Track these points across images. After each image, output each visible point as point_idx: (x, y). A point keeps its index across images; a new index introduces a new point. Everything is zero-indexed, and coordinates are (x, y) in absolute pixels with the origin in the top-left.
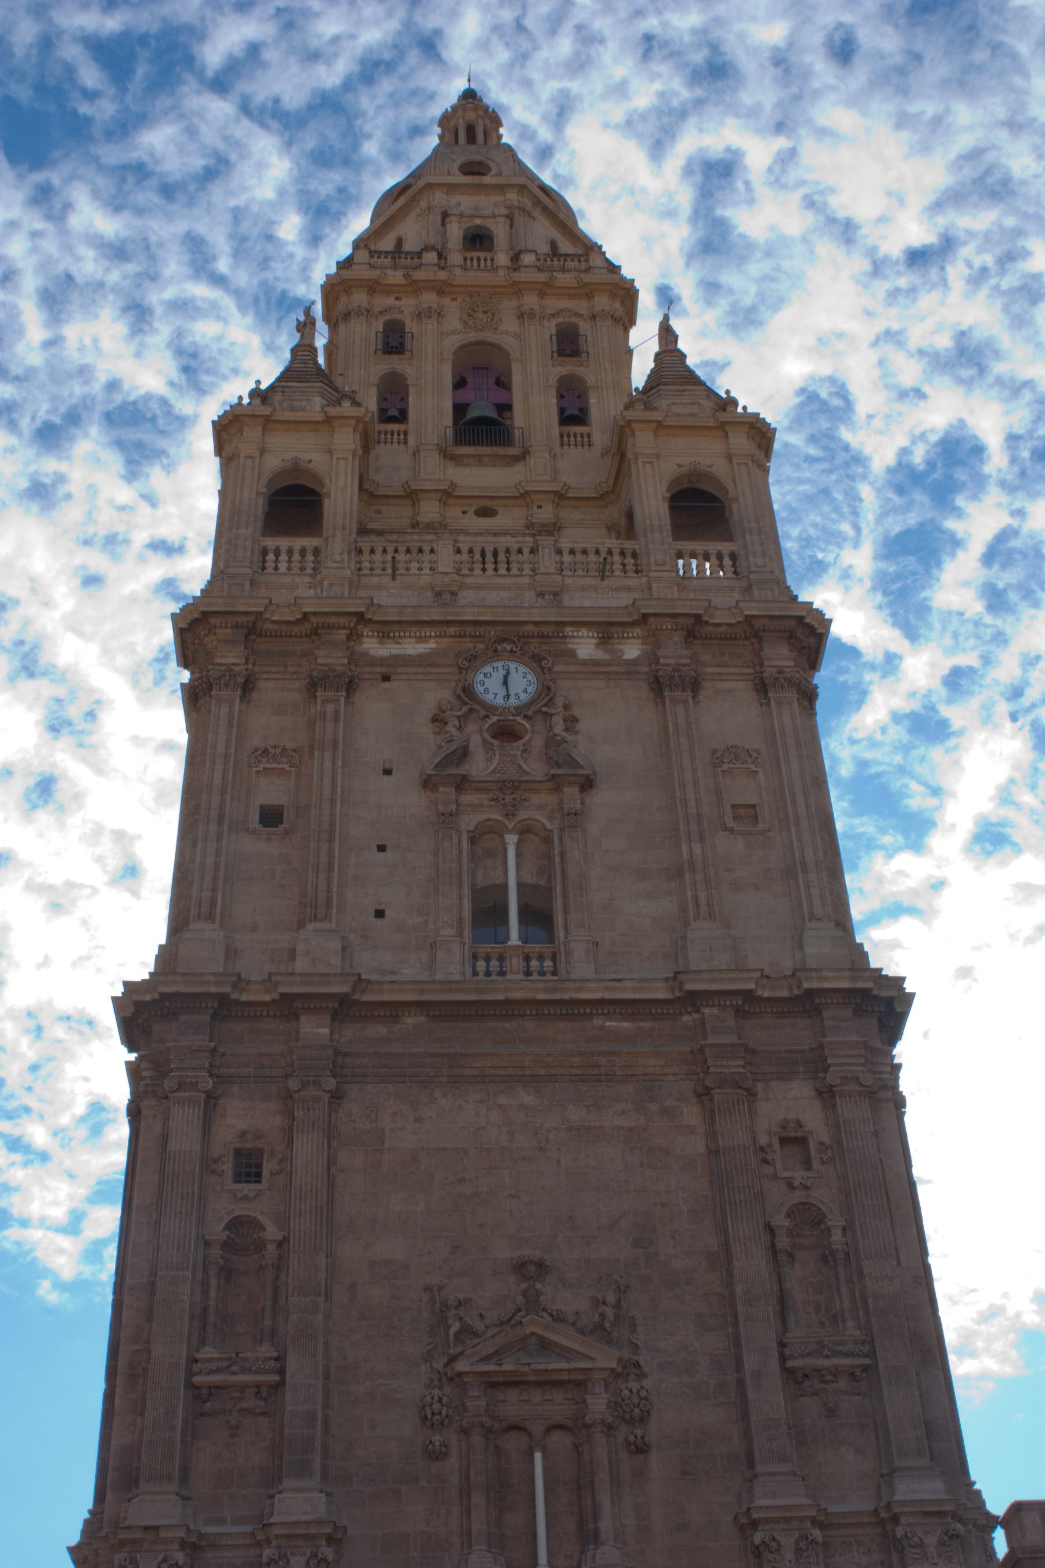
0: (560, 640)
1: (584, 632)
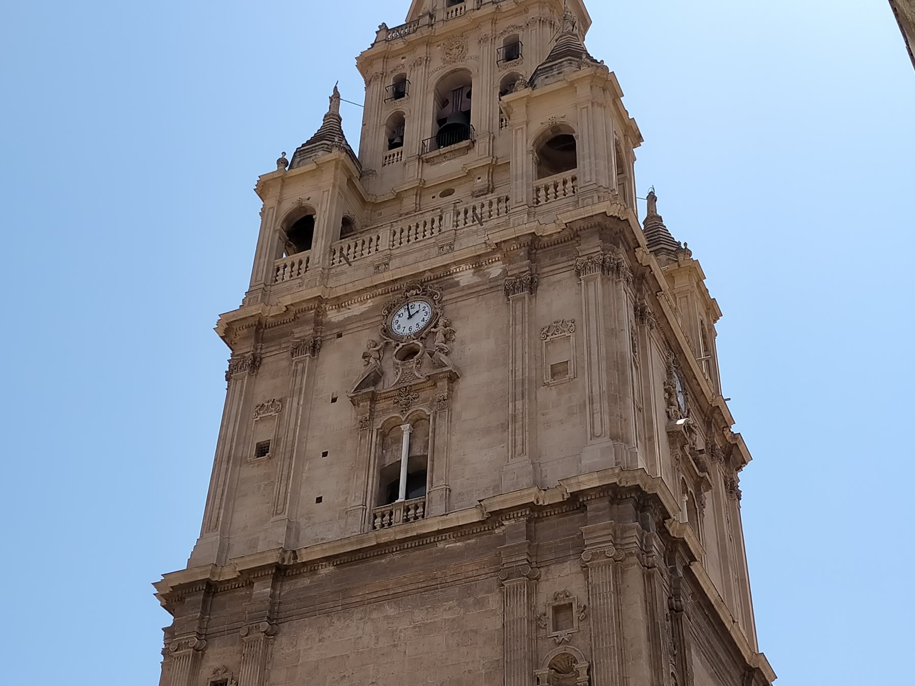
0: (449, 277)
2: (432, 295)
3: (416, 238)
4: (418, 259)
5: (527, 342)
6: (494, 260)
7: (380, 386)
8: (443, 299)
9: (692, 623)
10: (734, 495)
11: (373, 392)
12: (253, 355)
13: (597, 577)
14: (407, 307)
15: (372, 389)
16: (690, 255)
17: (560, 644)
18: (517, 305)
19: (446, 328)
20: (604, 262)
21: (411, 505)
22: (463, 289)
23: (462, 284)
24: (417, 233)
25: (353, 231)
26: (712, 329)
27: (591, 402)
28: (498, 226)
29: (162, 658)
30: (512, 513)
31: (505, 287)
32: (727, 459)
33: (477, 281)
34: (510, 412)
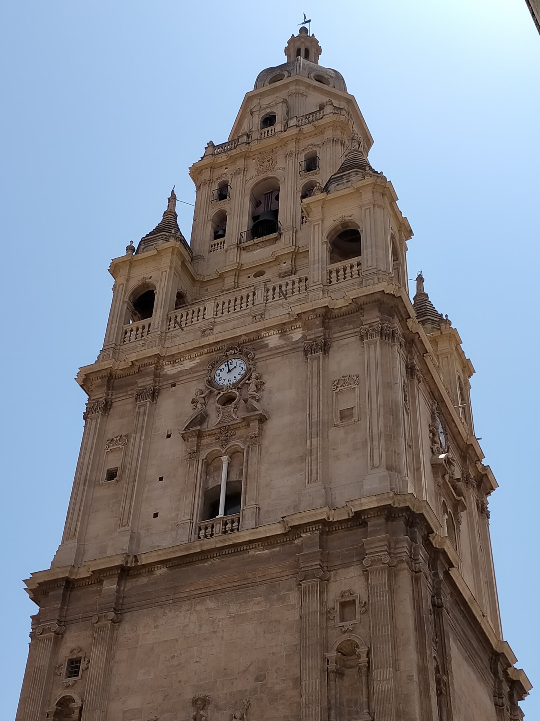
0: (261, 340)
1: (272, 332)
2: (247, 354)
3: (235, 309)
4: (236, 326)
5: (321, 392)
6: (295, 327)
8: (255, 358)
10: (484, 515)
11: (199, 430)
12: (105, 399)
13: (375, 579)
14: (227, 363)
15: (199, 427)
16: (450, 325)
17: (345, 632)
18: (313, 363)
19: (257, 380)
20: (382, 329)
21: (229, 520)
22: (271, 350)
23: (270, 346)
24: (235, 306)
25: (185, 303)
26: (467, 383)
27: (372, 439)
28: (299, 300)
29: (30, 640)
30: (308, 528)
31: (304, 349)
32: (479, 486)
33: (282, 343)
34: (307, 447)
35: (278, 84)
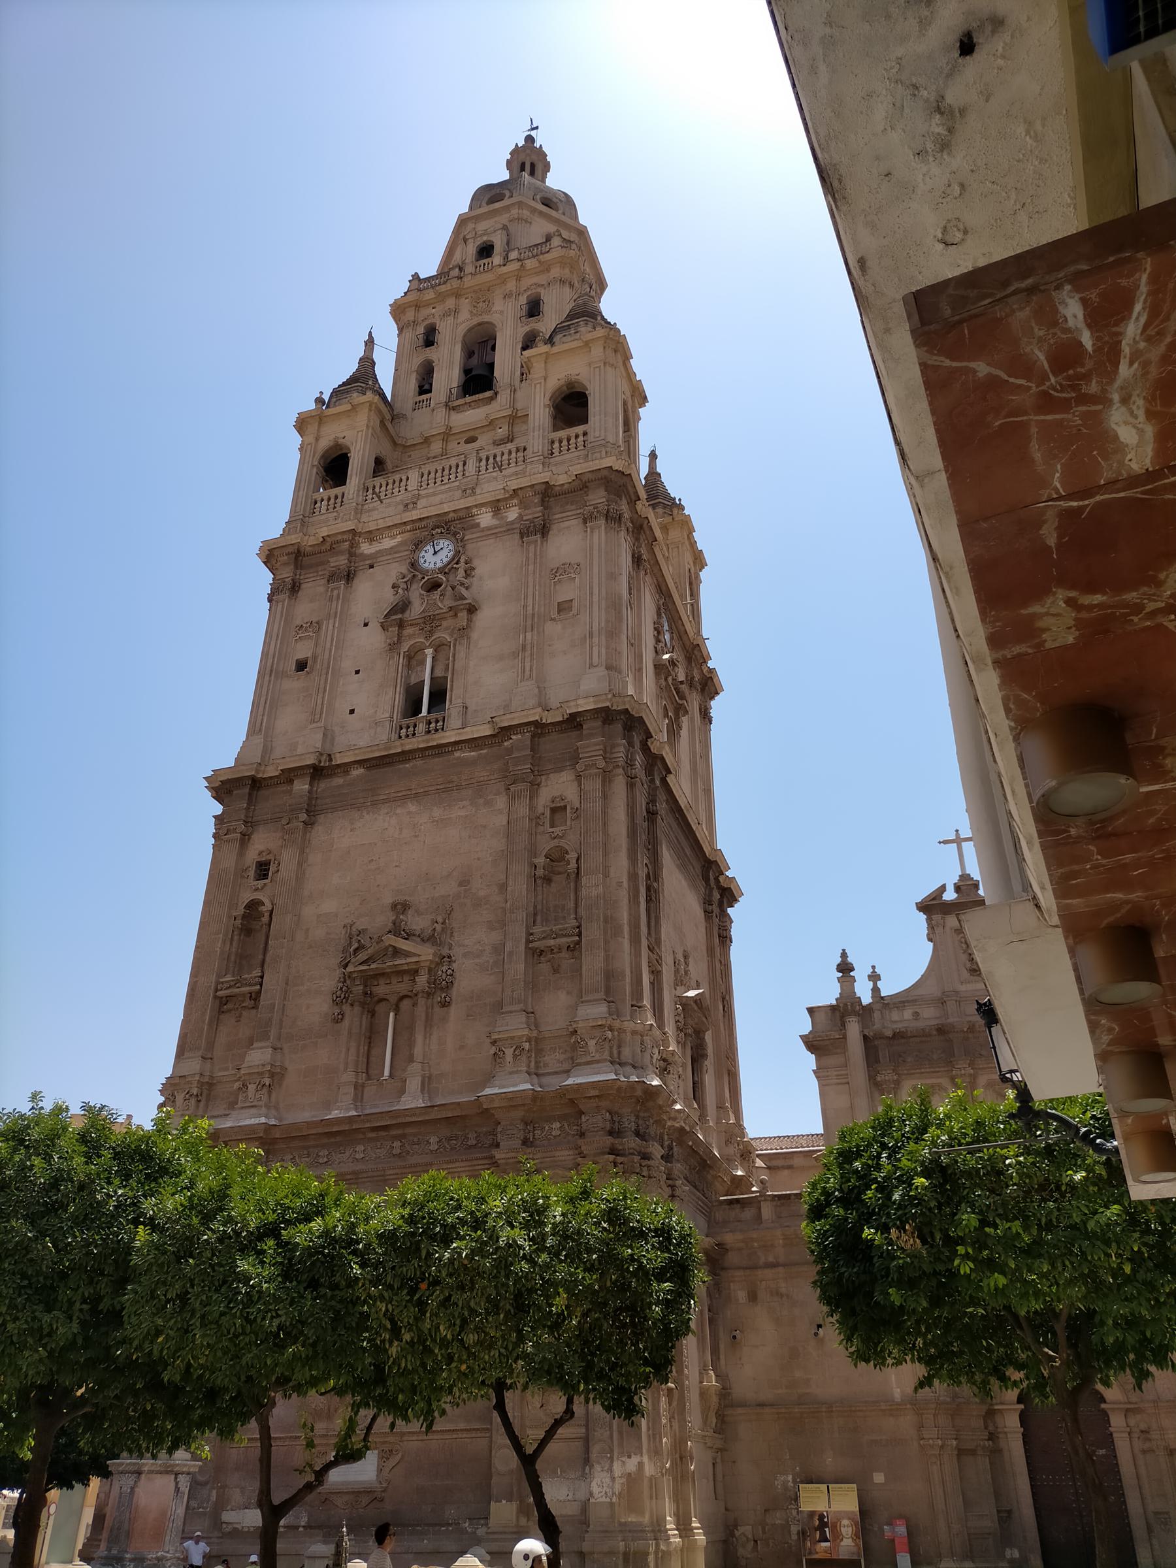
1: (484, 509)
2: (455, 534)
7: (407, 614)
9: (665, 823)
11: (401, 619)
12: (293, 580)
13: (588, 785)
15: (400, 616)
16: (683, 509)
20: (608, 512)
23: (482, 526)
26: (697, 577)
27: (591, 635)
28: (516, 474)
32: (703, 690)
35: (497, 205)
